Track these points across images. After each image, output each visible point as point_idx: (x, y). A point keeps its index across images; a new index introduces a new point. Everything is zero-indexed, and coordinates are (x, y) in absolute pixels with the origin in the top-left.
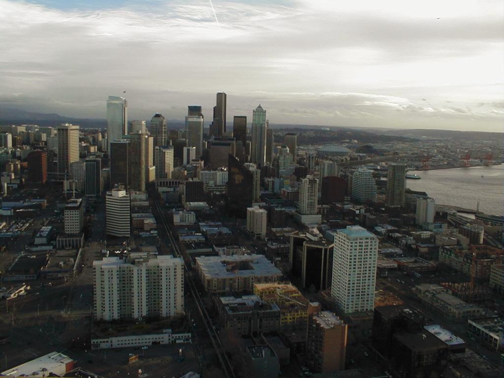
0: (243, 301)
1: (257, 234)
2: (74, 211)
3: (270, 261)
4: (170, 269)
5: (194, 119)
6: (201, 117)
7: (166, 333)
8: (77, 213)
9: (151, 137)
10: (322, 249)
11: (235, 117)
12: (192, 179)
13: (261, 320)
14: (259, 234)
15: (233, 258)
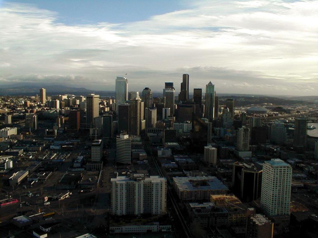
0: (204, 206)
1: (211, 163)
2: (97, 147)
3: (220, 181)
4: (158, 185)
5: (169, 91)
6: (173, 89)
7: (155, 225)
8: (99, 148)
9: (142, 102)
10: (254, 173)
11: (194, 89)
12: (169, 128)
13: (216, 219)
14: (212, 163)
15: (196, 178)
